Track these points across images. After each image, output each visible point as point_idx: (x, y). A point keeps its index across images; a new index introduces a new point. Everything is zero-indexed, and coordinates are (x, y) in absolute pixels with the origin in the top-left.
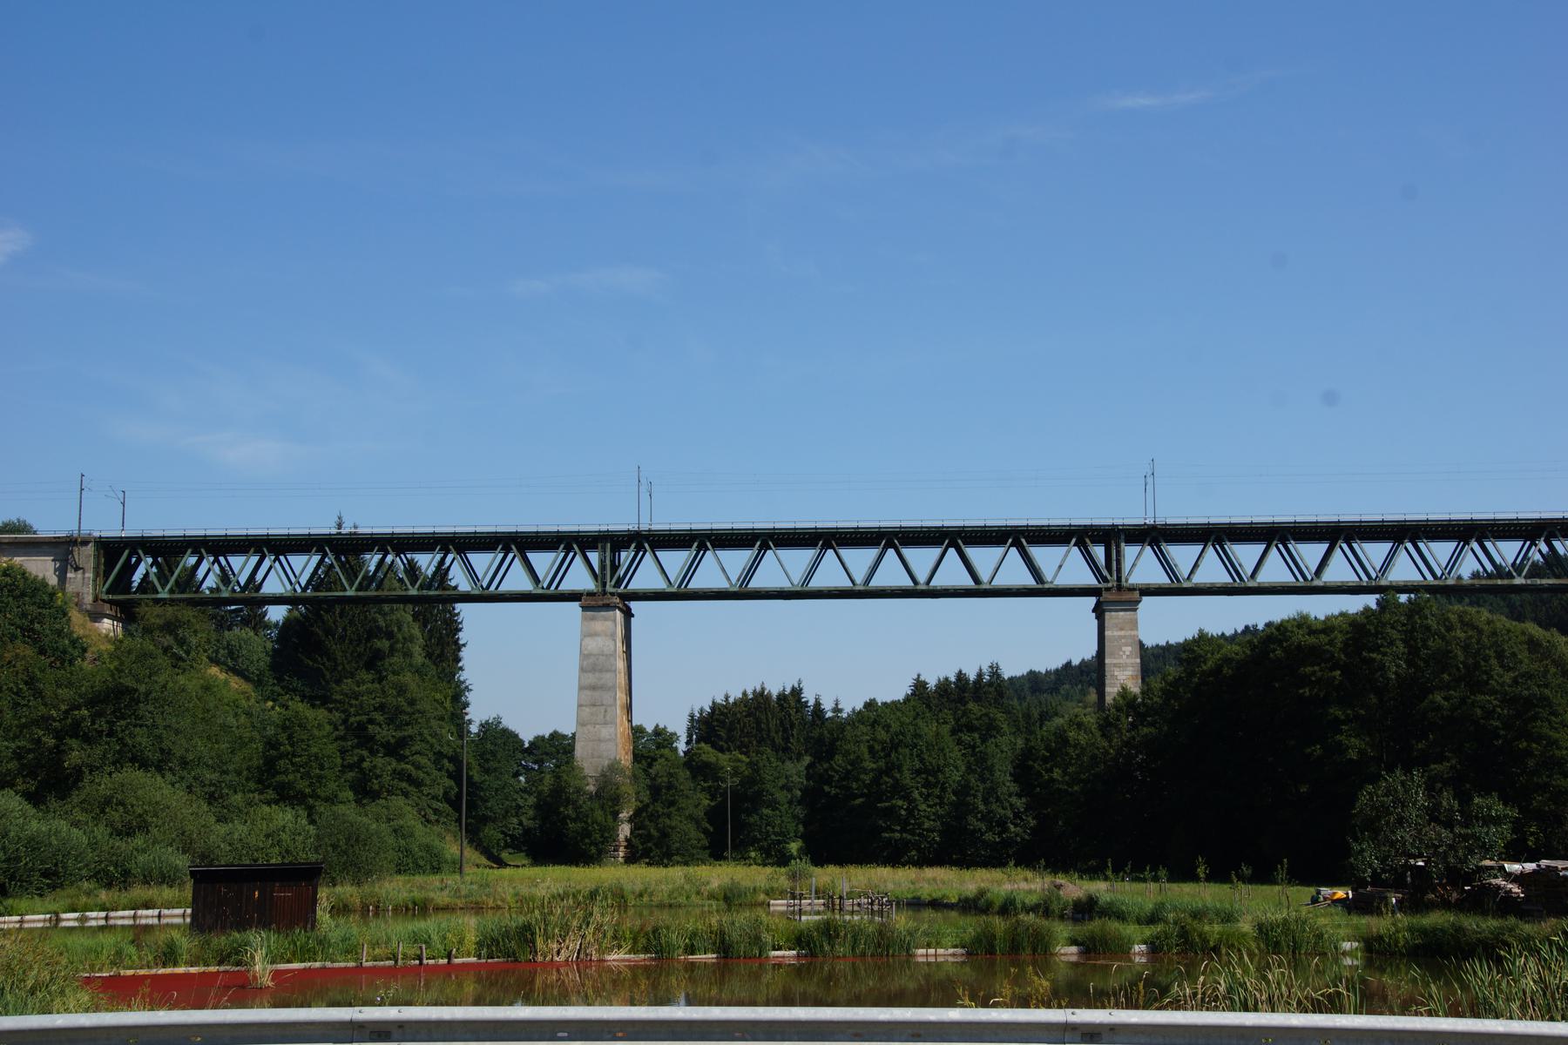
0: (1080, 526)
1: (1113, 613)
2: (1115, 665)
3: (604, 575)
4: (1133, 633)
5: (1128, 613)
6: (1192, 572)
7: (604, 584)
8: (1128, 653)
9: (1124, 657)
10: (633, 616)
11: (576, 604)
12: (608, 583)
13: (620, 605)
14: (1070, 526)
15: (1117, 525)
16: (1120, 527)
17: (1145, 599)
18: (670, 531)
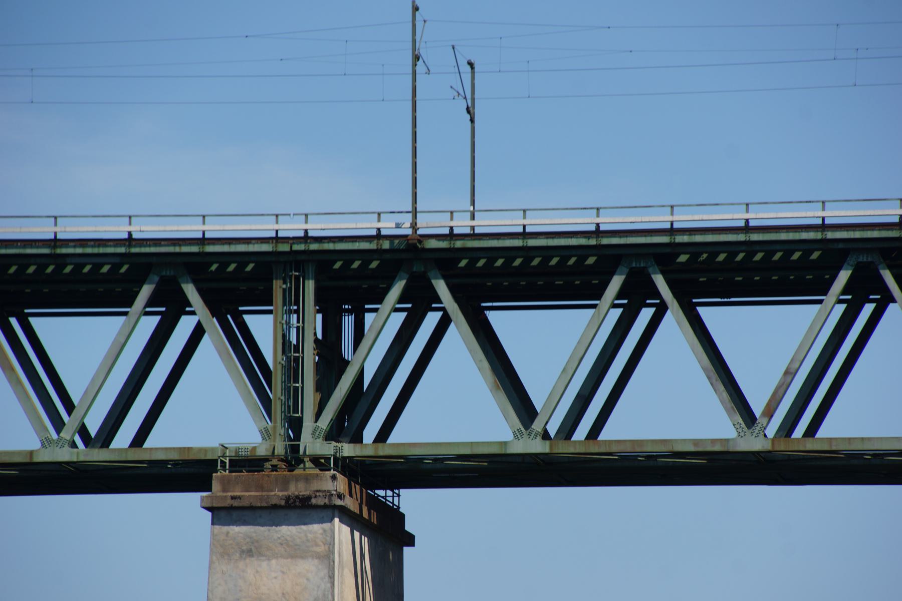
3: (294, 396)
7: (296, 425)
10: (409, 540)
11: (192, 500)
12: (308, 425)
13: (350, 503)
18: (524, 235)
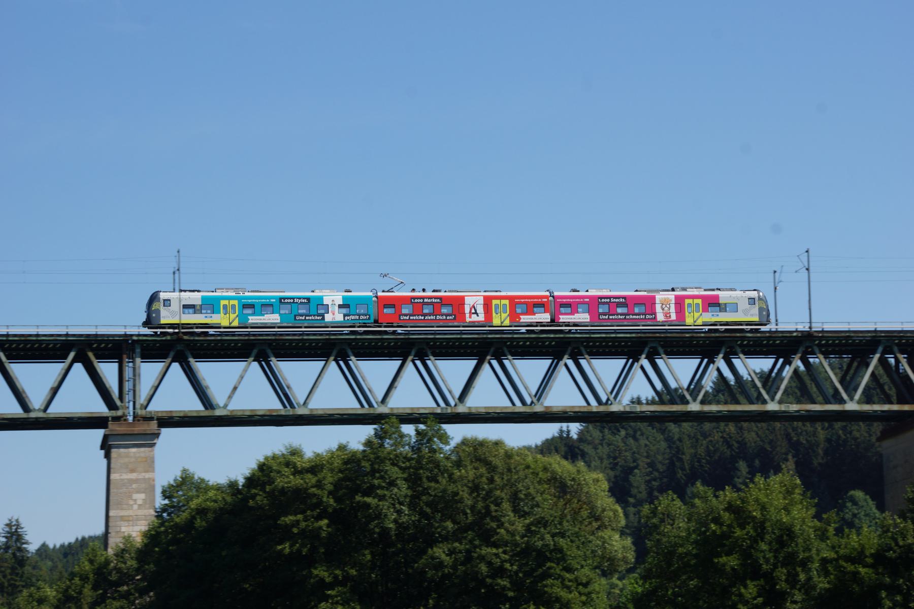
0: (81, 336)
1: (122, 450)
2: (122, 518)
4: (147, 475)
5: (142, 449)
6: (230, 397)
8: (139, 502)
9: (135, 507)
14: (67, 335)
15: (132, 335)
16: (135, 338)
17: (164, 431)
